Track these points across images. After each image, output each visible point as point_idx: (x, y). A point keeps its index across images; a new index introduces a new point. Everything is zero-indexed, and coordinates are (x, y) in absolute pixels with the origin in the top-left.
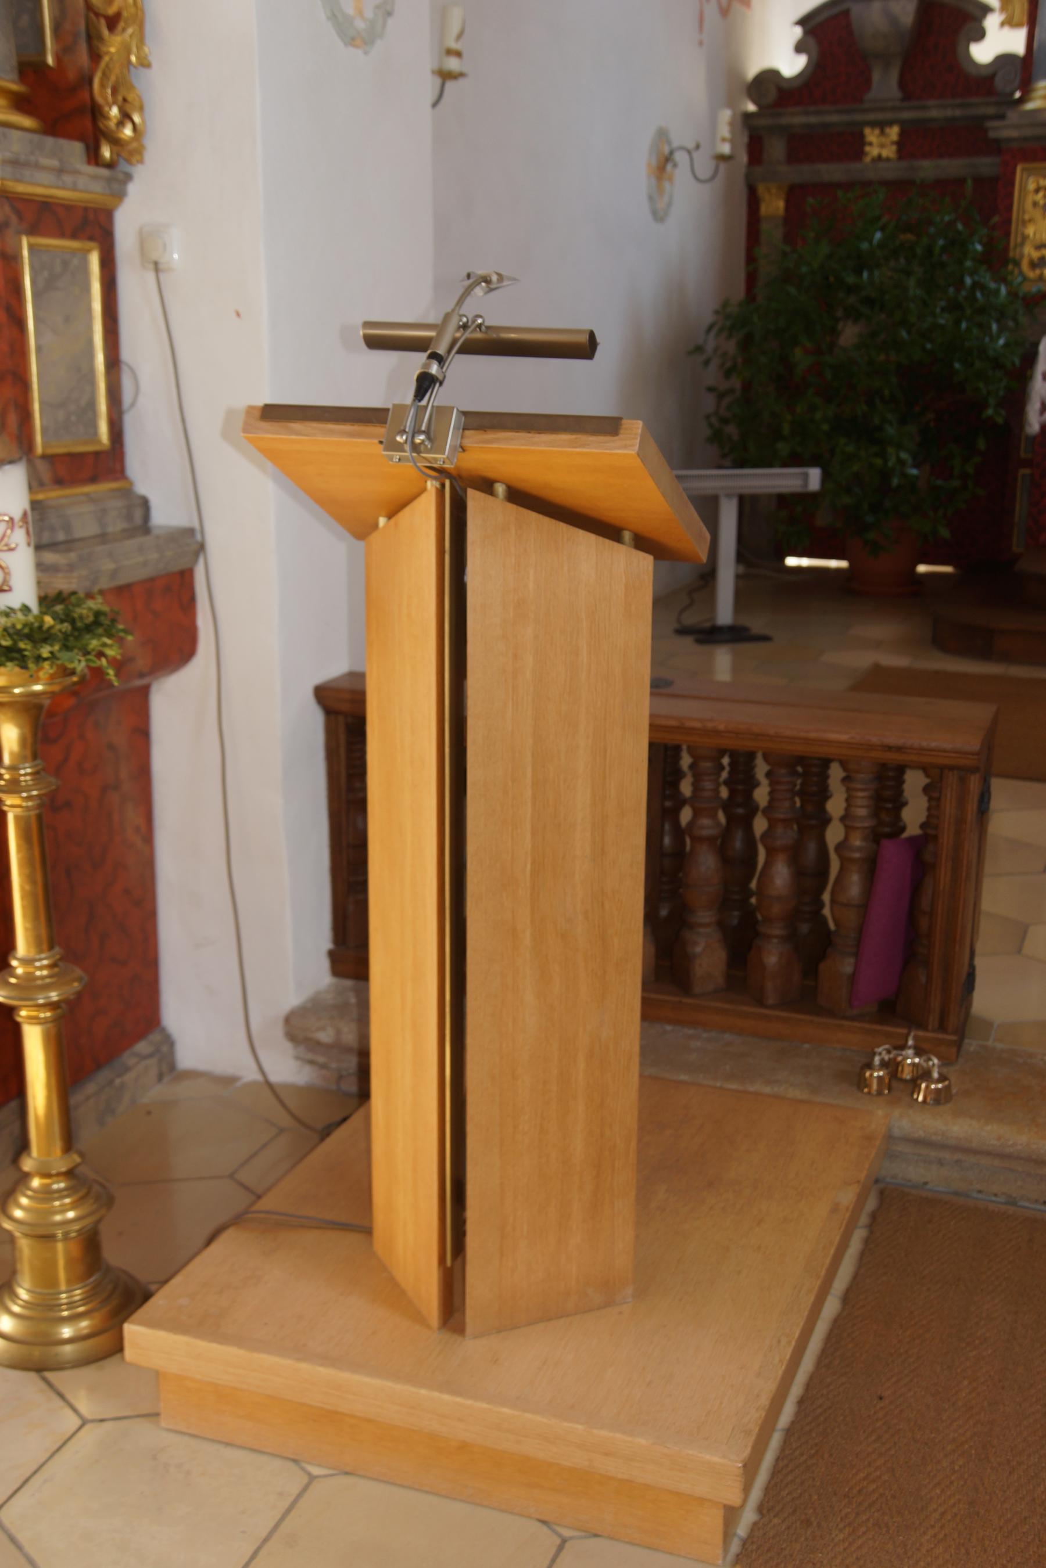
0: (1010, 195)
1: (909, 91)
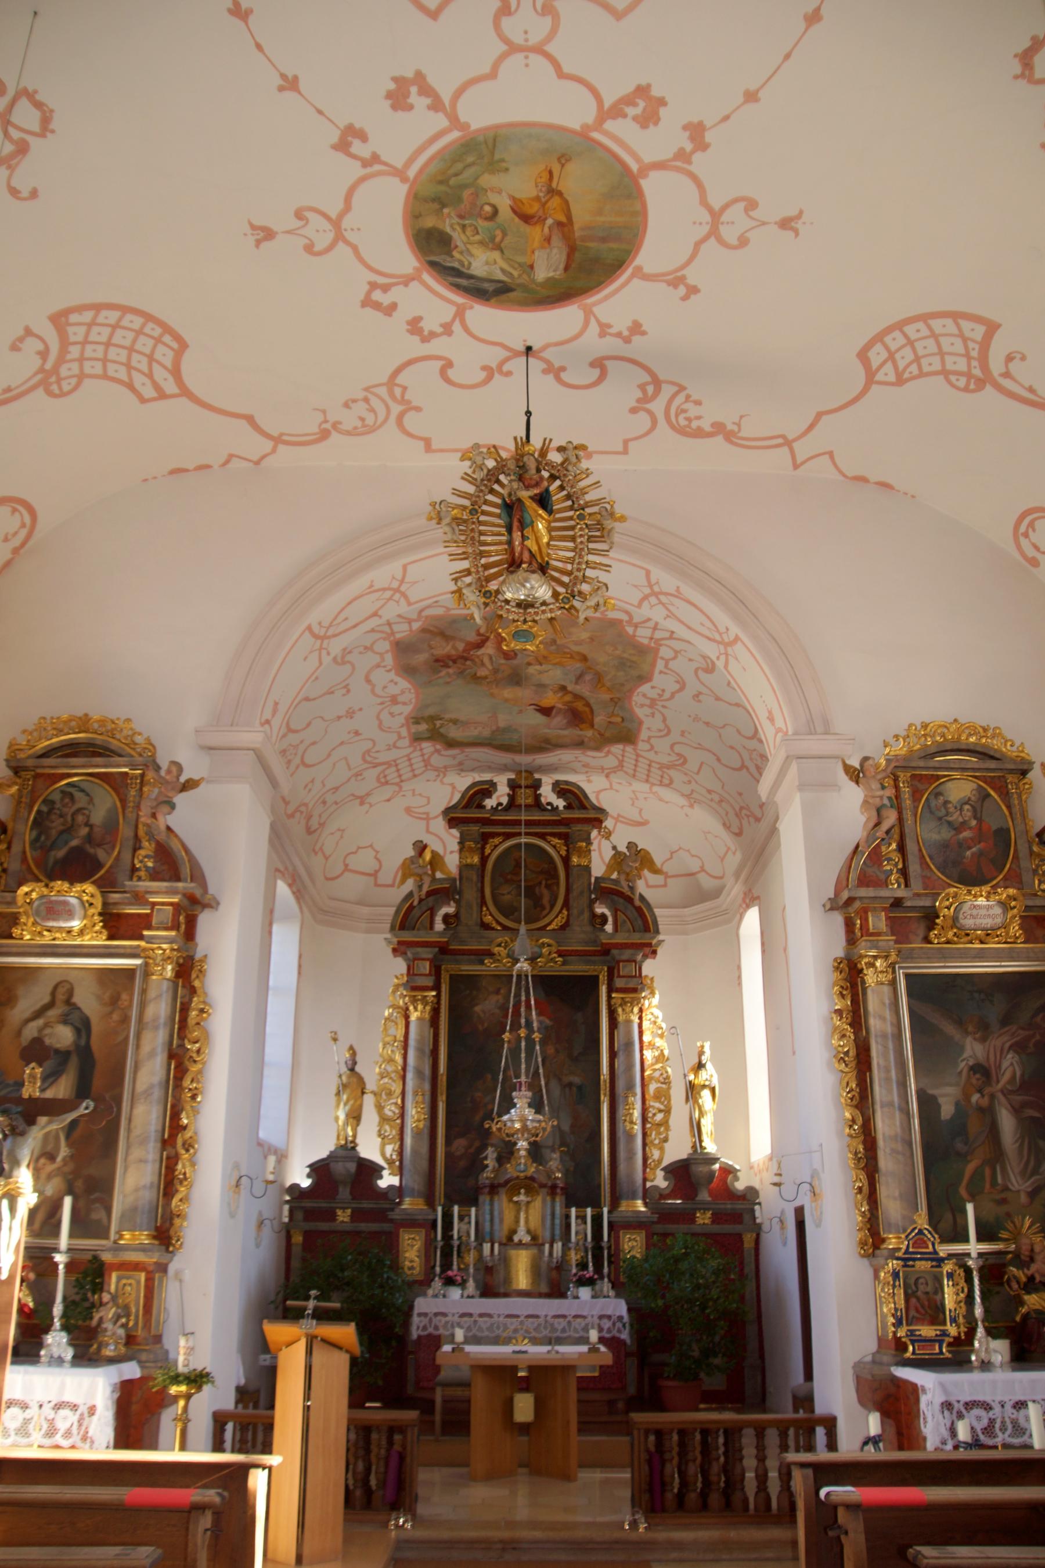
0: (398, 1241)
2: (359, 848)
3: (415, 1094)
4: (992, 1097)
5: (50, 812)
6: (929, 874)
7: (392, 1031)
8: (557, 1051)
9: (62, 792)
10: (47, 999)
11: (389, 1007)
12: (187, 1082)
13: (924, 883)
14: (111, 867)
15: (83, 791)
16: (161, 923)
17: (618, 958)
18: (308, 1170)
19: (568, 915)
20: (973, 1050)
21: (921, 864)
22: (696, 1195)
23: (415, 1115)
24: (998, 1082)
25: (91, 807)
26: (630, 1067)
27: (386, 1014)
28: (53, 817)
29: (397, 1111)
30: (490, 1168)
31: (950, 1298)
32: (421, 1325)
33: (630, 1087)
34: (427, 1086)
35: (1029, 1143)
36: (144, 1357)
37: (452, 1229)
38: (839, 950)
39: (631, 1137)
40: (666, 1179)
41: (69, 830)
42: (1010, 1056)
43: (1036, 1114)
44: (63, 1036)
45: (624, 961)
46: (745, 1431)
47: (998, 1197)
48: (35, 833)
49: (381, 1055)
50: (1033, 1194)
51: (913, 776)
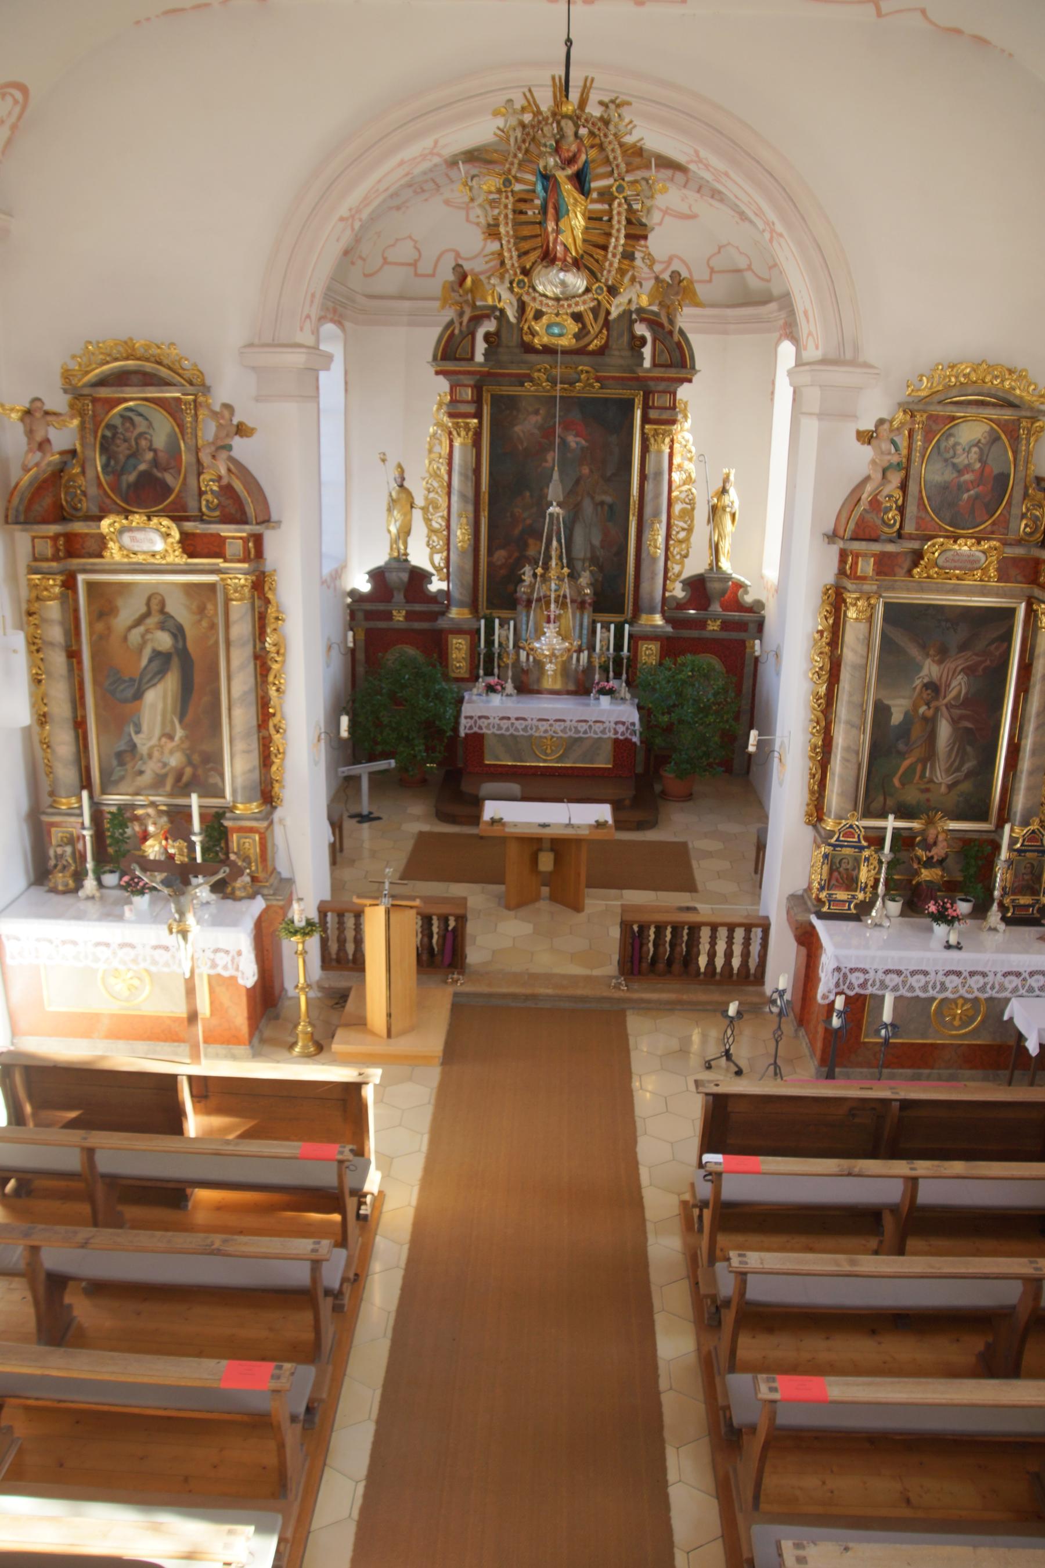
0: (447, 645)
1: (408, 601)
2: (397, 240)
3: (460, 516)
4: (937, 709)
5: (114, 435)
6: (923, 515)
7: (437, 449)
8: (591, 471)
9: (122, 416)
10: (143, 609)
11: (435, 425)
12: (271, 678)
13: (917, 523)
14: (180, 491)
15: (141, 415)
16: (234, 555)
17: (653, 389)
18: (367, 577)
19: (608, 336)
20: (930, 670)
21: (919, 505)
22: (709, 605)
23: (461, 535)
24: (945, 697)
25: (151, 431)
26: (657, 496)
27: (431, 430)
28: (118, 442)
29: (444, 524)
30: (527, 583)
31: (864, 875)
32: (468, 725)
33: (657, 514)
34: (470, 508)
35: (958, 750)
36: (265, 891)
37: (493, 634)
38: (829, 577)
39: (654, 559)
40: (683, 590)
41: (135, 455)
42: (960, 677)
43: (969, 725)
44: (164, 641)
45: (659, 392)
46: (703, 928)
47: (923, 787)
48: (104, 458)
49: (428, 471)
50: (951, 787)
51: (930, 417)
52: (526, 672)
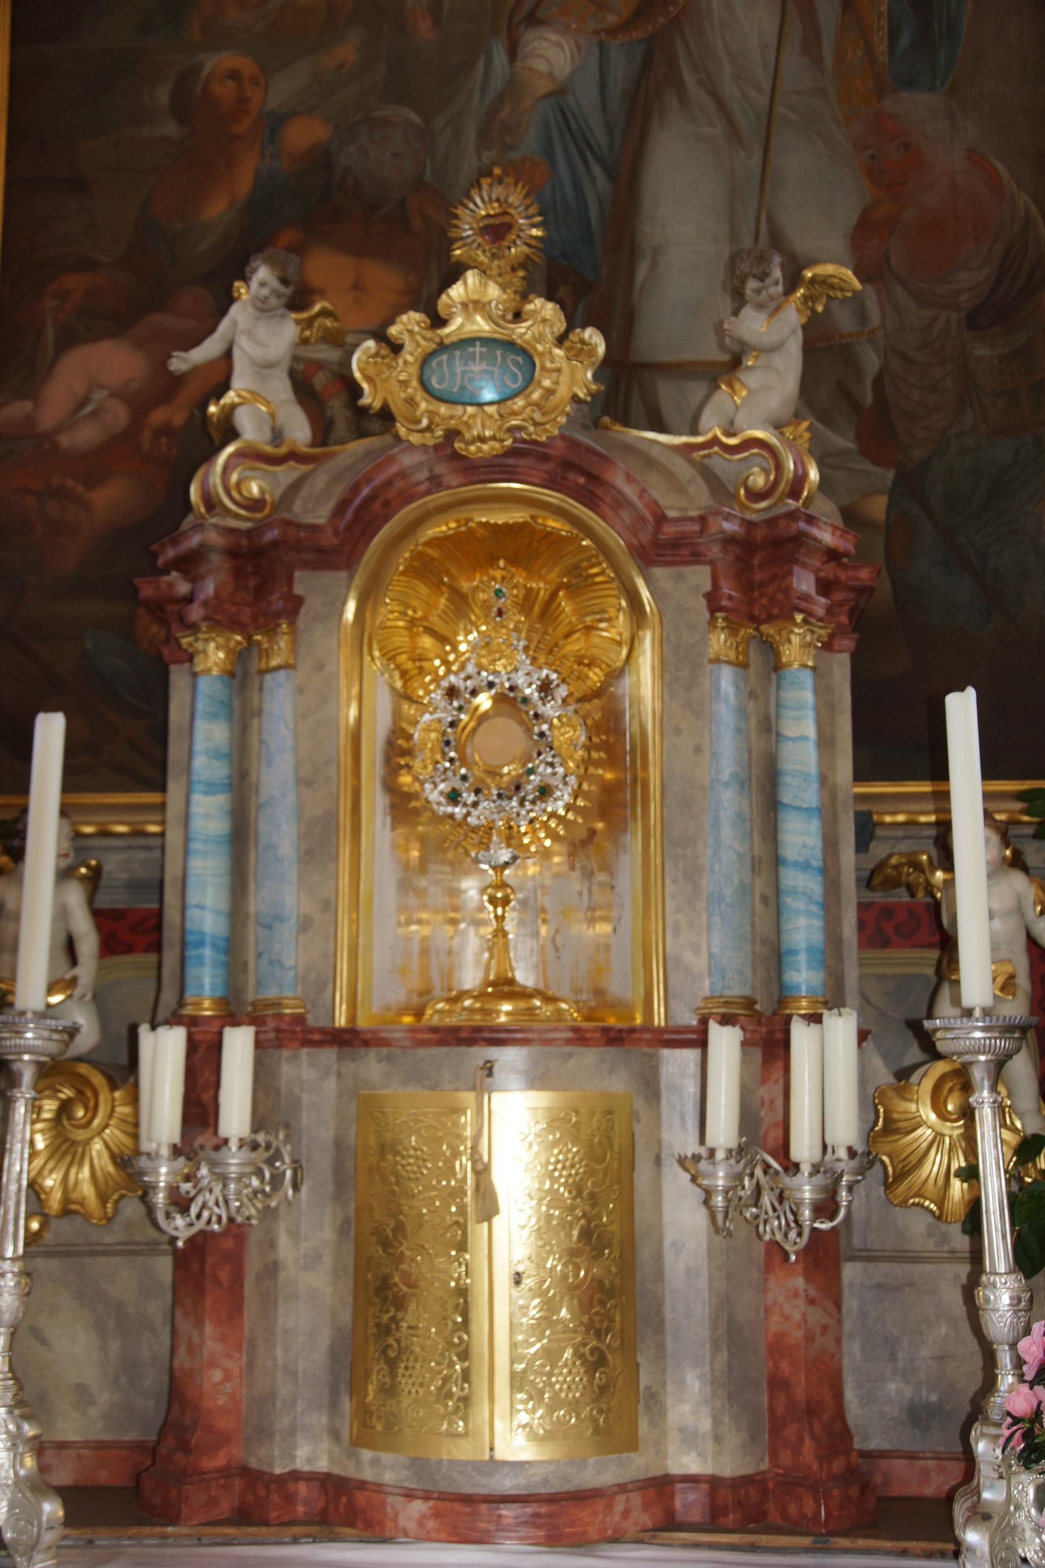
52: (210, 1270)
